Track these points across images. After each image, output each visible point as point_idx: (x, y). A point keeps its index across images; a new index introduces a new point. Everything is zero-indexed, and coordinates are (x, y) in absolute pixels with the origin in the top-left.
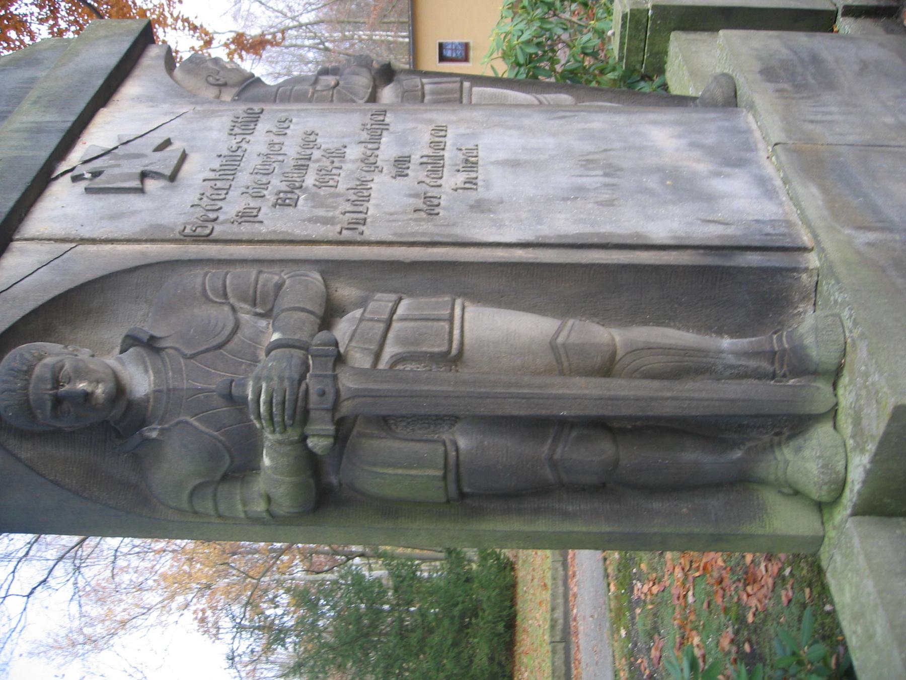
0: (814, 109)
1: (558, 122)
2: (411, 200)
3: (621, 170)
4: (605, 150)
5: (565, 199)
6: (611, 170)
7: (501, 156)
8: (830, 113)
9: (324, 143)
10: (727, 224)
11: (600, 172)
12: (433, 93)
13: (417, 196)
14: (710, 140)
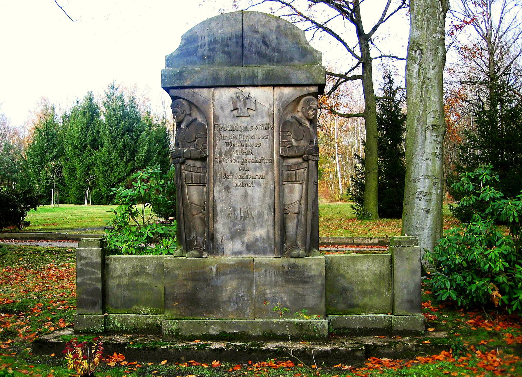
0: (273, 273)
1: (268, 207)
3: (244, 220)
4: (253, 218)
5: (230, 207)
6: (243, 218)
7: (250, 192)
8: (271, 277)
9: (255, 149)
11: (242, 215)
12: (291, 174)
13: (231, 173)
14: (259, 244)
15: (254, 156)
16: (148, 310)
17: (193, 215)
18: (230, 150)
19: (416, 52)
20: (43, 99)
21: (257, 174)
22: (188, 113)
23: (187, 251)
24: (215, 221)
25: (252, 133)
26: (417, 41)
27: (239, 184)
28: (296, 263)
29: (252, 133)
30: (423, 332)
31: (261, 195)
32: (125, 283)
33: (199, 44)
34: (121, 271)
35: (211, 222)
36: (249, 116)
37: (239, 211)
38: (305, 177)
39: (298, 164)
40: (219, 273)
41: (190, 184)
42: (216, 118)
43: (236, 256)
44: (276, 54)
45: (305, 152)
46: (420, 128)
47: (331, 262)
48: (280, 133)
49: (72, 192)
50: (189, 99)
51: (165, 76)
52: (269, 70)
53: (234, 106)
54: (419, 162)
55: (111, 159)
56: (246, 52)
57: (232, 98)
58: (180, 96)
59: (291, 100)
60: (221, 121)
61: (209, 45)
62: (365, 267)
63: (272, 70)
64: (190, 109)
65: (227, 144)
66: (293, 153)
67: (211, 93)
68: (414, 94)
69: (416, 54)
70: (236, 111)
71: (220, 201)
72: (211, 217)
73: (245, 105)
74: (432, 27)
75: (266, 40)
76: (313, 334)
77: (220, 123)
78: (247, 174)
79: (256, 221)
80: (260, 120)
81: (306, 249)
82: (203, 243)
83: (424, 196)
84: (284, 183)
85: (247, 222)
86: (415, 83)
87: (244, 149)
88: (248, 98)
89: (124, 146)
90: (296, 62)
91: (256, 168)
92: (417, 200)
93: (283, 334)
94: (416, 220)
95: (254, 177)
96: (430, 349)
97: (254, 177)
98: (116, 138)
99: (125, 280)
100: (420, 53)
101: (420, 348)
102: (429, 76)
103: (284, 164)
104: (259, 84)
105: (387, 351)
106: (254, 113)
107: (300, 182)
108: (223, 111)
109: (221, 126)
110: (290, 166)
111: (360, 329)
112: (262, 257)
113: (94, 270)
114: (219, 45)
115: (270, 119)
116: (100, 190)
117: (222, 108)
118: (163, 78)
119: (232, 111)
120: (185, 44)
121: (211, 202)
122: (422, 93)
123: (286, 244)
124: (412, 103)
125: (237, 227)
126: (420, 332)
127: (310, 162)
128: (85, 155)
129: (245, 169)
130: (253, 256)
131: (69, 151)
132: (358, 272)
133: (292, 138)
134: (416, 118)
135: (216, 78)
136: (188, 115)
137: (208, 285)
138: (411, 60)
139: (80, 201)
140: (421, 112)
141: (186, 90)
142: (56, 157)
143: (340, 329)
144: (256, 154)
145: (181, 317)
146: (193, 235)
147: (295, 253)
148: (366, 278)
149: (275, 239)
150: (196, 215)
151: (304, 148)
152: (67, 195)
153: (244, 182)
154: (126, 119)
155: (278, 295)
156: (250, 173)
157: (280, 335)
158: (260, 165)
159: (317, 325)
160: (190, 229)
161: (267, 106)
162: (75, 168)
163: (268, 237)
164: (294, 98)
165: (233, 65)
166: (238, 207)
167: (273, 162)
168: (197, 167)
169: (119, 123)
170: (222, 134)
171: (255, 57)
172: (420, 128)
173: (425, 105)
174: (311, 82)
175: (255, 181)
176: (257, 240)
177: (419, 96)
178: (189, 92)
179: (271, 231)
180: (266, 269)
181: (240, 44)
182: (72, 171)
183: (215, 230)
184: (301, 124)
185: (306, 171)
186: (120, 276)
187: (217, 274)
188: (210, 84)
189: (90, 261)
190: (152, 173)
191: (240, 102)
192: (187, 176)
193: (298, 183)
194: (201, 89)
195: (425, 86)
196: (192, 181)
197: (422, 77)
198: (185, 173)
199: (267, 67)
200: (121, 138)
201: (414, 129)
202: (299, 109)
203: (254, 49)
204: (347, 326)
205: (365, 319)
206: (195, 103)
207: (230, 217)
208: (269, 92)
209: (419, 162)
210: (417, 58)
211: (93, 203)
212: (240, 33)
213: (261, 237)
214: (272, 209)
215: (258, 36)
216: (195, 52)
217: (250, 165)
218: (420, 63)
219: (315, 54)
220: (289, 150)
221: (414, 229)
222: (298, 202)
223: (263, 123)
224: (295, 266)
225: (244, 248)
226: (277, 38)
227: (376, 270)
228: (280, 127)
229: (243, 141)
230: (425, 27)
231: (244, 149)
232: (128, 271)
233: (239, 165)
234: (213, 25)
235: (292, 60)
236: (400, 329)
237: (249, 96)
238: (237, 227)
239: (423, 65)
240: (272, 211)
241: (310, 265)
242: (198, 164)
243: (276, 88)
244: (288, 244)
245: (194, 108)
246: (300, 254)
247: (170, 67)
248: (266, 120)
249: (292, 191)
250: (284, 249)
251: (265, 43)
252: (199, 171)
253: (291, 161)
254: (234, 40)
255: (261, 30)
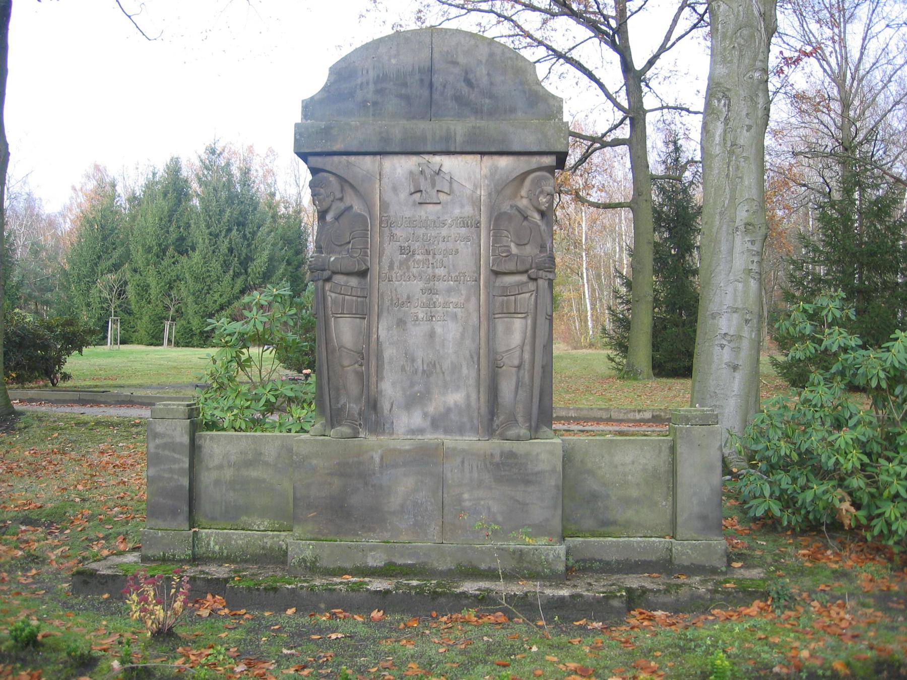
2: (405, 296)
4: (443, 373)
5: (406, 354)
6: (427, 374)
7: (439, 330)
8: (471, 472)
9: (448, 259)
10: (390, 411)
11: (425, 368)
12: (508, 302)
13: (408, 297)
14: (453, 416)
15: (446, 270)
16: (266, 523)
17: (343, 367)
18: (407, 260)
19: (719, 101)
20: (97, 168)
21: (452, 300)
22: (339, 195)
23: (333, 427)
24: (380, 377)
25: (444, 232)
26: (721, 83)
27: (421, 316)
28: (514, 450)
29: (444, 232)
30: (724, 569)
31: (458, 336)
32: (228, 478)
33: (359, 81)
34: (221, 457)
35: (373, 379)
36: (440, 203)
37: (420, 361)
38: (532, 306)
39: (521, 284)
40: (385, 465)
41: (339, 316)
42: (384, 206)
43: (414, 437)
44: (487, 101)
45: (531, 266)
46: (725, 228)
47: (573, 448)
48: (492, 232)
49: (143, 325)
50: (340, 172)
51: (301, 135)
52: (474, 128)
53: (414, 186)
54: (722, 284)
55: (208, 271)
56: (436, 96)
57: (411, 173)
58: (324, 168)
59: (511, 178)
60: (393, 210)
61: (375, 83)
62: (628, 459)
63: (479, 128)
64: (342, 190)
65: (402, 250)
66: (511, 266)
67: (377, 164)
68: (716, 171)
69: (720, 105)
70: (418, 194)
71: (390, 344)
72: (373, 370)
73: (433, 184)
74: (747, 61)
75: (471, 76)
76: (540, 568)
77: (392, 213)
78: (435, 300)
79: (448, 378)
80: (459, 211)
81: (530, 426)
82: (360, 414)
83: (730, 341)
84: (497, 316)
85: (433, 379)
86: (718, 152)
87: (430, 257)
88: (439, 172)
89: (231, 250)
90: (520, 114)
91: (449, 291)
92: (717, 349)
93: (490, 567)
94: (715, 382)
95: (446, 305)
96: (734, 597)
97: (446, 305)
98: (217, 236)
99: (228, 474)
100: (727, 102)
101: (718, 596)
102: (741, 141)
103: (497, 284)
104: (458, 150)
105: (663, 599)
106: (449, 198)
107: (523, 315)
108: (397, 195)
109: (393, 219)
110: (507, 287)
111: (618, 562)
112: (457, 438)
113: (176, 456)
114: (392, 83)
115: (474, 210)
116: (189, 323)
117: (395, 189)
118: (298, 137)
119: (411, 194)
120: (335, 82)
121: (373, 345)
122: (728, 170)
123: (498, 418)
124: (712, 187)
125: (416, 388)
126: (719, 568)
127: (540, 282)
128: (165, 263)
129: (432, 291)
130: (442, 436)
131: (139, 257)
132: (616, 467)
133: (511, 241)
134: (718, 211)
135: (386, 140)
136: (337, 199)
137: (366, 484)
138: (711, 114)
139: (155, 339)
140: (727, 202)
141: (336, 159)
142: (116, 267)
143: (584, 561)
144: (451, 267)
145: (320, 537)
146: (343, 400)
147: (512, 432)
148: (630, 477)
149: (479, 409)
150: (349, 366)
151: (530, 258)
152: (133, 330)
153: (429, 314)
154: (234, 204)
155: (482, 502)
156: (440, 299)
157: (485, 570)
158: (457, 285)
159: (547, 555)
160: (338, 390)
161: (469, 186)
162: (149, 286)
163: (468, 406)
164: (514, 175)
165: (414, 118)
166: (420, 354)
167: (477, 280)
168: (352, 288)
169: (222, 212)
170: (394, 231)
171: (451, 104)
172: (725, 228)
173: (733, 191)
174: (544, 148)
175: (447, 312)
176: (449, 410)
177: (723, 175)
178: (340, 162)
179: (474, 396)
180: (463, 459)
181: (427, 83)
182: (144, 289)
183: (379, 392)
184: (526, 218)
185: (533, 297)
186: (220, 467)
187: (381, 466)
188: (376, 149)
189: (170, 440)
190: (276, 296)
191: (426, 179)
192: (334, 302)
193: (520, 316)
194: (361, 157)
195: (734, 158)
196: (343, 309)
197: (729, 144)
198: (331, 296)
199: (472, 122)
200: (225, 236)
201: (714, 230)
202: (523, 193)
203: (450, 92)
204: (597, 557)
205: (627, 546)
206: (349, 180)
207: (405, 371)
208: (474, 163)
209: (722, 284)
210: (721, 112)
211: (177, 344)
212: (428, 64)
213: (456, 404)
214: (476, 359)
215: (456, 70)
216: (352, 94)
217: (440, 285)
218: (727, 119)
219: (551, 102)
220: (505, 261)
221: (711, 397)
222: (518, 349)
223: (463, 216)
224: (512, 455)
225: (428, 423)
226: (489, 74)
227: (646, 464)
228: (490, 221)
229: (429, 244)
230: (735, 61)
231: (430, 257)
232: (233, 458)
233: (421, 284)
234: (382, 50)
235: (513, 110)
236: (686, 564)
237: (440, 170)
238: (416, 388)
239: (731, 123)
240: (476, 362)
241: (537, 454)
242: (354, 281)
243: (485, 158)
244: (502, 418)
245: (348, 190)
246: (521, 435)
247: (309, 119)
248: (468, 210)
249: (508, 330)
250: (495, 427)
251: (469, 83)
252: (354, 294)
253: (509, 280)
254: (417, 77)
255: (462, 60)
